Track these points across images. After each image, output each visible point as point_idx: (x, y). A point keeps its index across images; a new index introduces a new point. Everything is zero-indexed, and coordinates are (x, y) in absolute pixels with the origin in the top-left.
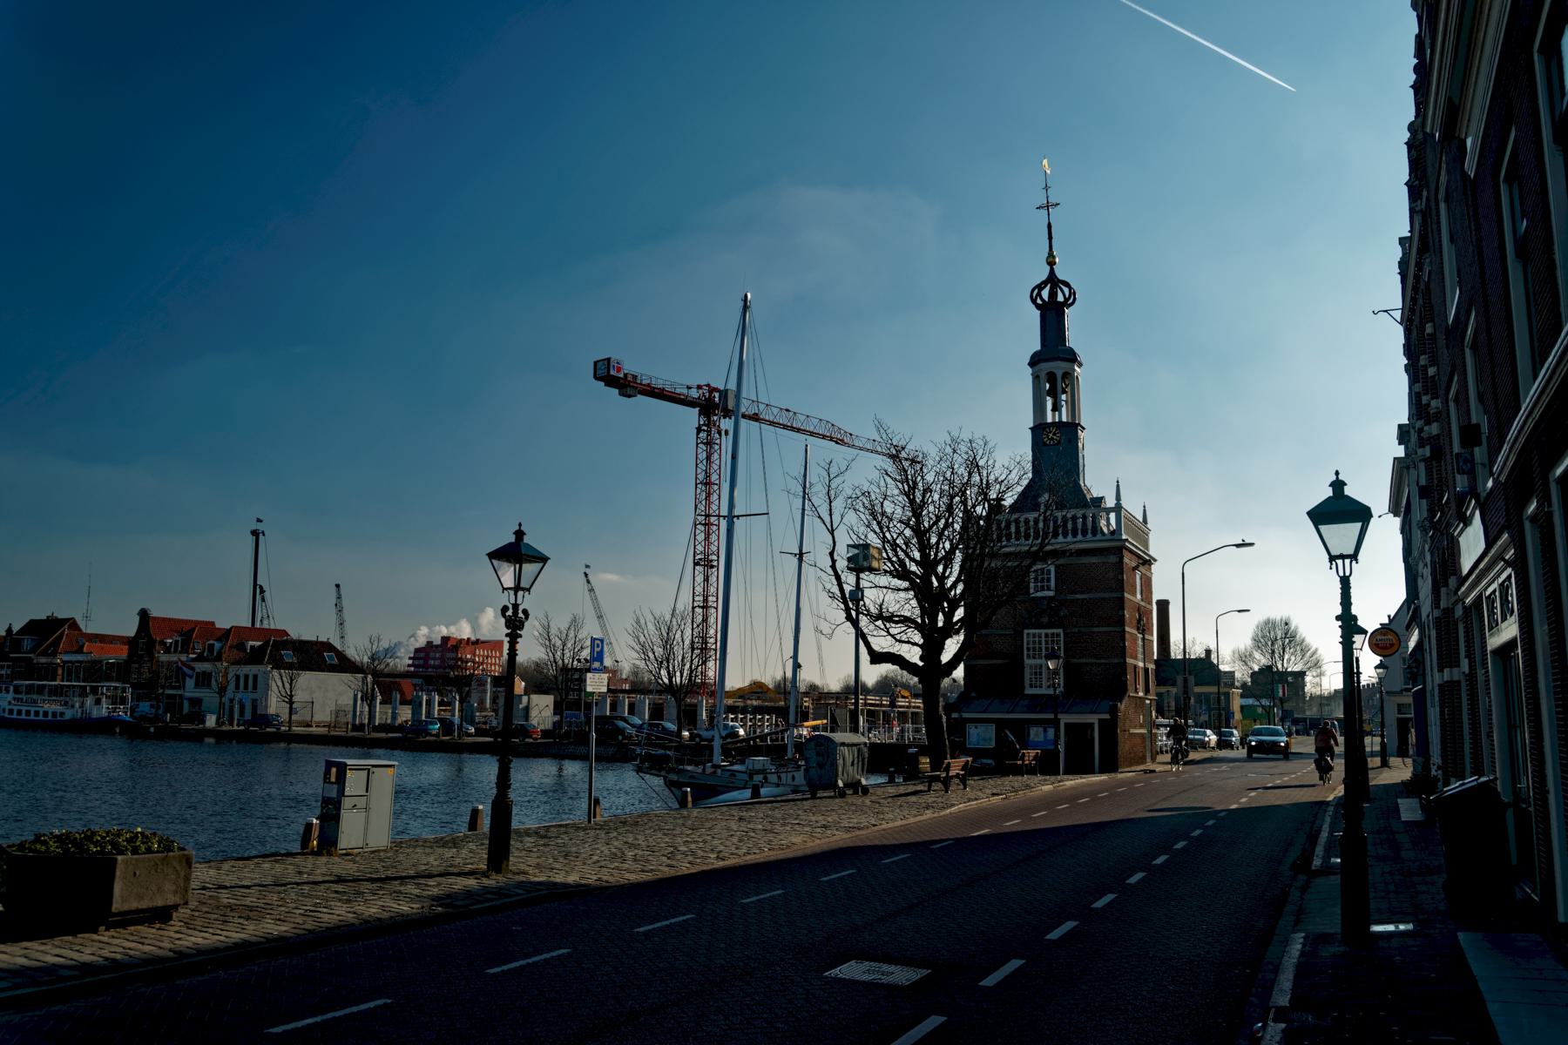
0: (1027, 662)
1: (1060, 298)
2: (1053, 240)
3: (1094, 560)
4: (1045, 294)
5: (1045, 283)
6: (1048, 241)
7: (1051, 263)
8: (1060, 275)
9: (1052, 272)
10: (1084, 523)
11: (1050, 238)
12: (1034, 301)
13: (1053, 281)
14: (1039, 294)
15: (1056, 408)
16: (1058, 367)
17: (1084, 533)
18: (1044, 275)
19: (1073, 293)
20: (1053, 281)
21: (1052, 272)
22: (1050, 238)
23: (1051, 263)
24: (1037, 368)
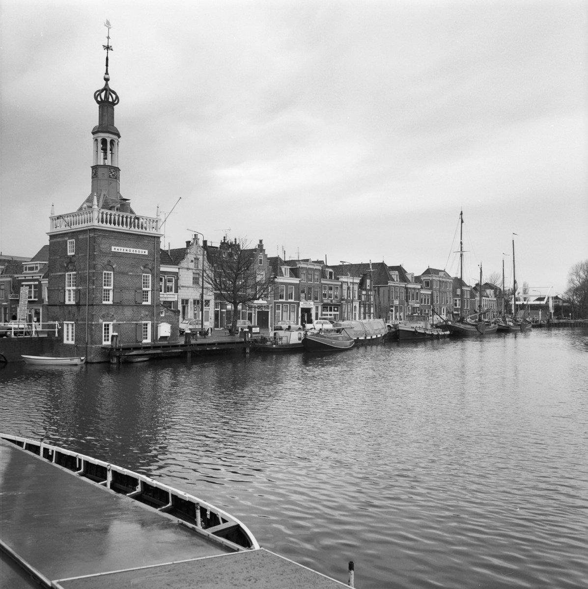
0: (67, 288)
1: (110, 100)
2: (108, 67)
3: (59, 240)
4: (103, 95)
5: (102, 91)
6: (105, 67)
7: (107, 80)
8: (112, 86)
9: (107, 84)
10: (110, 218)
11: (107, 65)
12: (96, 98)
13: (106, 89)
14: (100, 94)
15: (105, 158)
16: (109, 137)
17: (106, 222)
18: (102, 85)
19: (117, 97)
20: (106, 89)
21: (107, 84)
22: (107, 65)
23: (107, 80)
24: (96, 135)
